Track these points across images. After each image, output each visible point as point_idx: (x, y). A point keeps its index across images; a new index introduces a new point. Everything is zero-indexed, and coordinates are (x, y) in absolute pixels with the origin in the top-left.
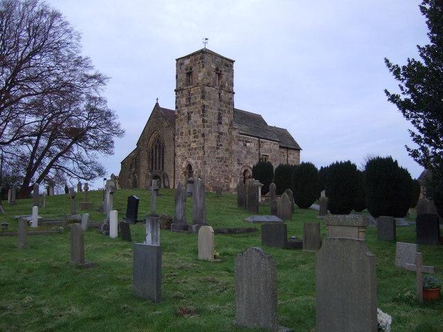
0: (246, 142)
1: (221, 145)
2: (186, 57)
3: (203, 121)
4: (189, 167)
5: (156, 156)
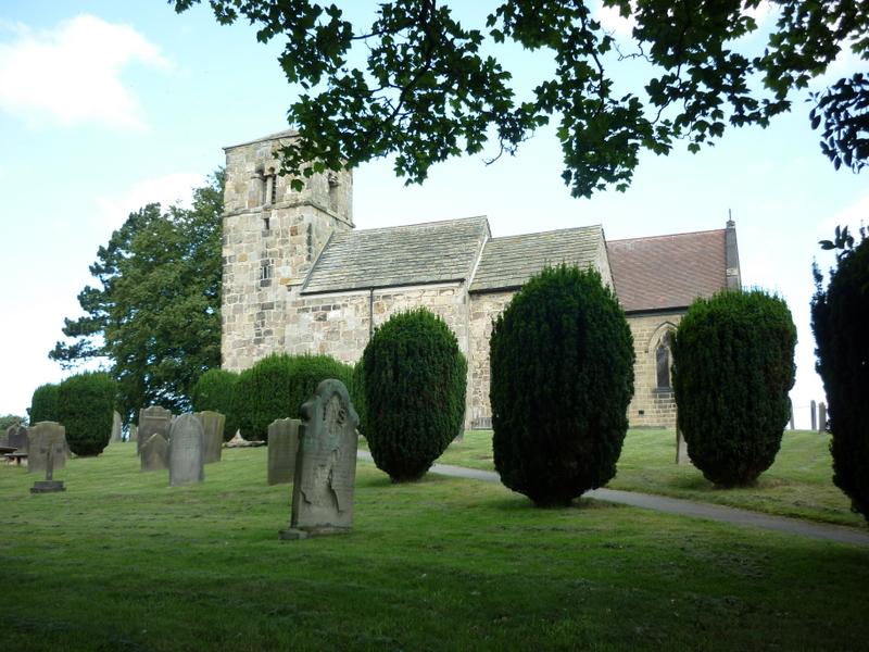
0: (328, 308)
1: (269, 332)
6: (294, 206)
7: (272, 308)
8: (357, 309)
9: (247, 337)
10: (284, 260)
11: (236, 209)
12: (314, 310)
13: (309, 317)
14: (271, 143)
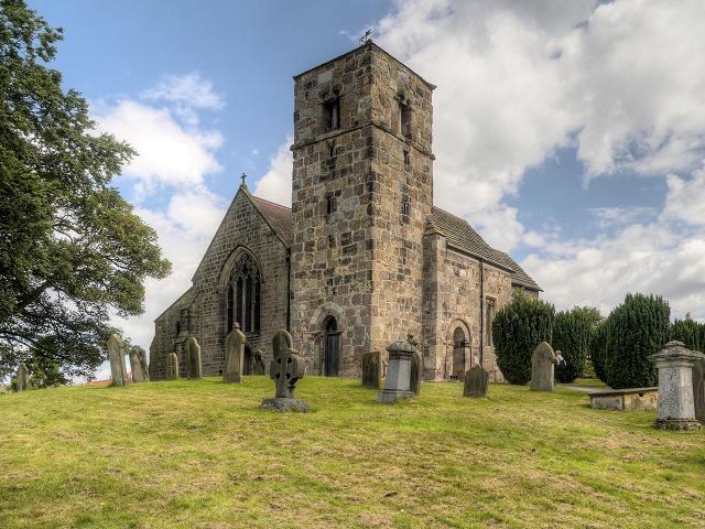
0: (460, 266)
1: (408, 271)
2: (323, 65)
3: (370, 211)
4: (330, 323)
5: (240, 302)
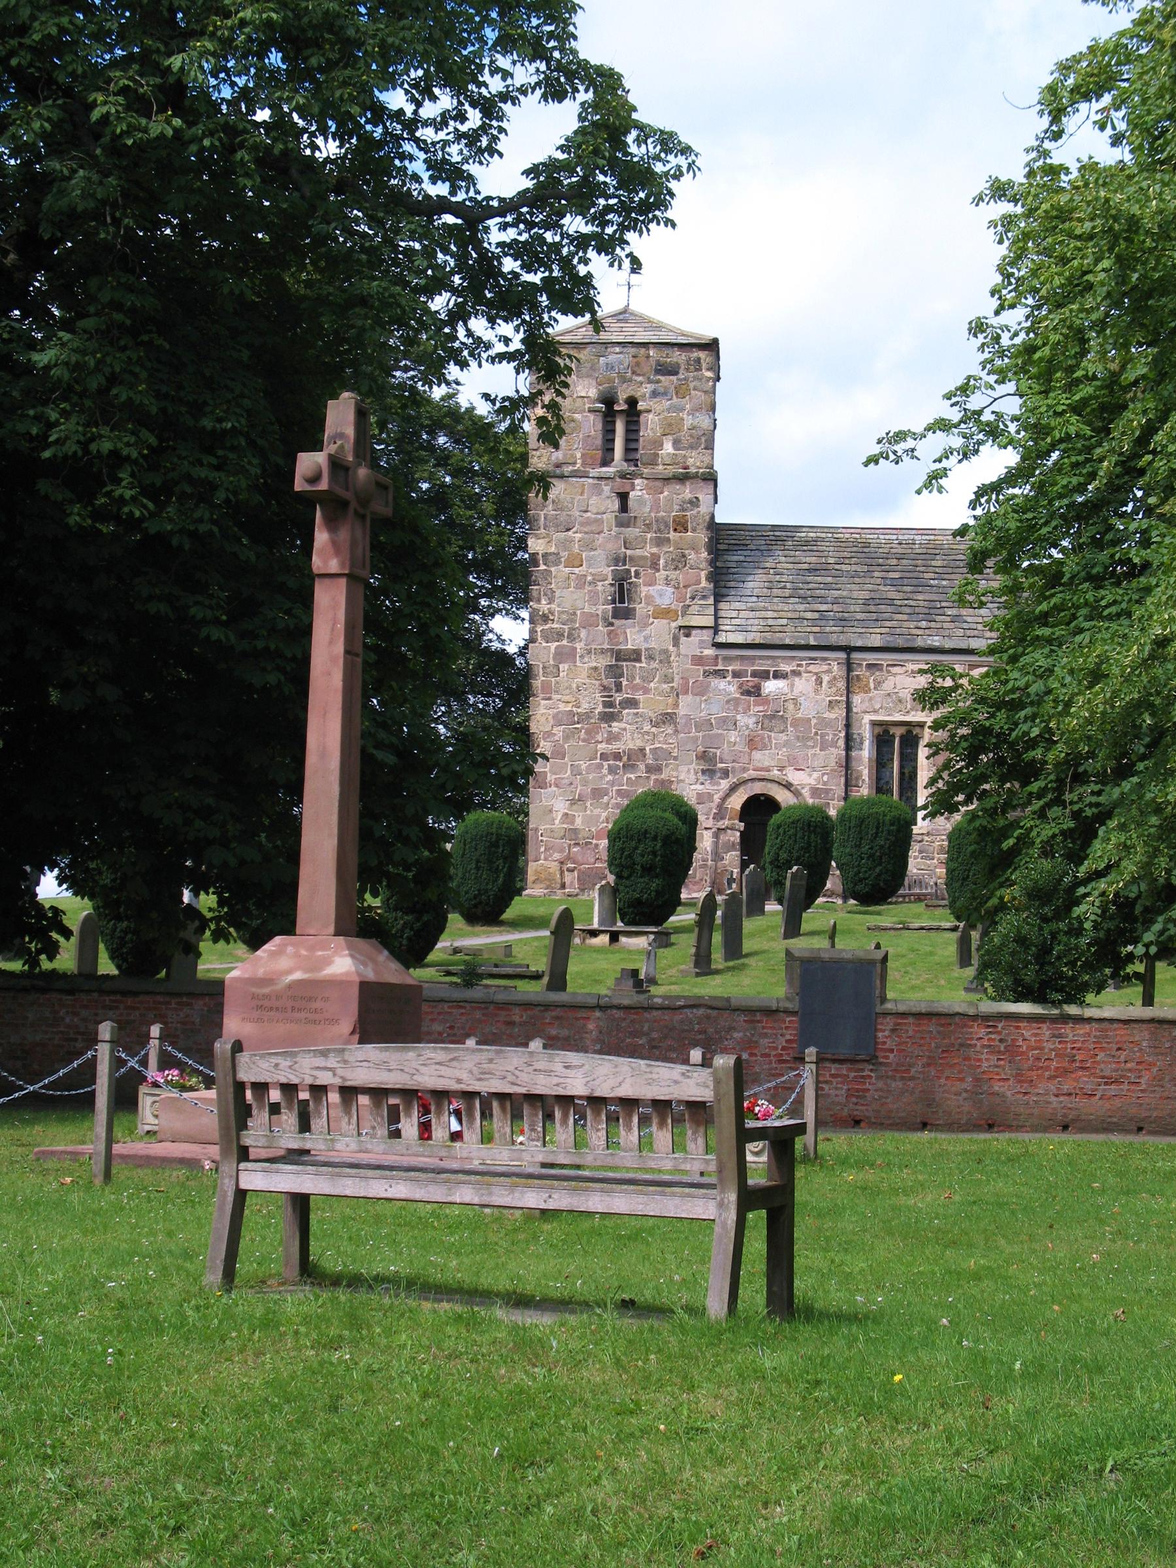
0: (765, 675)
1: (632, 703)
6: (683, 478)
7: (639, 660)
8: (819, 682)
9: (585, 707)
10: (661, 575)
11: (558, 466)
12: (736, 675)
13: (728, 687)
14: (633, 350)
